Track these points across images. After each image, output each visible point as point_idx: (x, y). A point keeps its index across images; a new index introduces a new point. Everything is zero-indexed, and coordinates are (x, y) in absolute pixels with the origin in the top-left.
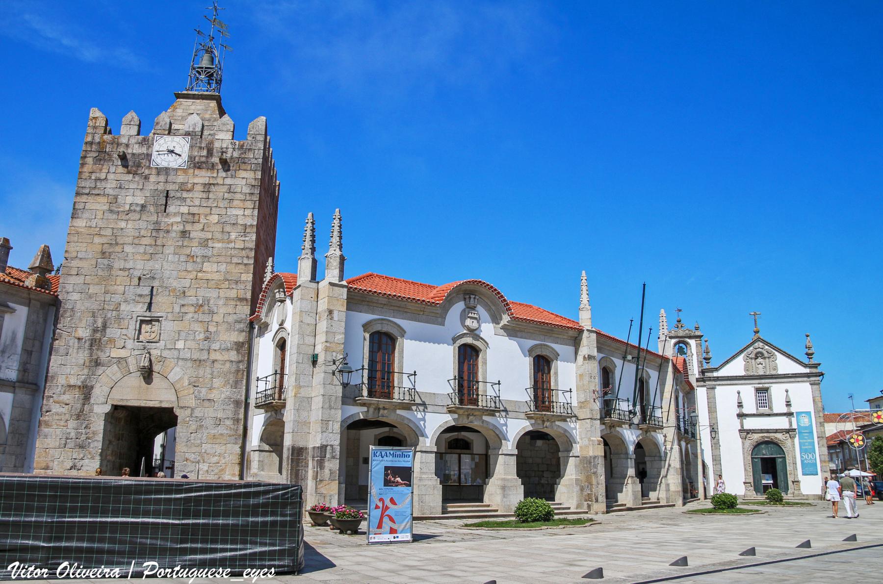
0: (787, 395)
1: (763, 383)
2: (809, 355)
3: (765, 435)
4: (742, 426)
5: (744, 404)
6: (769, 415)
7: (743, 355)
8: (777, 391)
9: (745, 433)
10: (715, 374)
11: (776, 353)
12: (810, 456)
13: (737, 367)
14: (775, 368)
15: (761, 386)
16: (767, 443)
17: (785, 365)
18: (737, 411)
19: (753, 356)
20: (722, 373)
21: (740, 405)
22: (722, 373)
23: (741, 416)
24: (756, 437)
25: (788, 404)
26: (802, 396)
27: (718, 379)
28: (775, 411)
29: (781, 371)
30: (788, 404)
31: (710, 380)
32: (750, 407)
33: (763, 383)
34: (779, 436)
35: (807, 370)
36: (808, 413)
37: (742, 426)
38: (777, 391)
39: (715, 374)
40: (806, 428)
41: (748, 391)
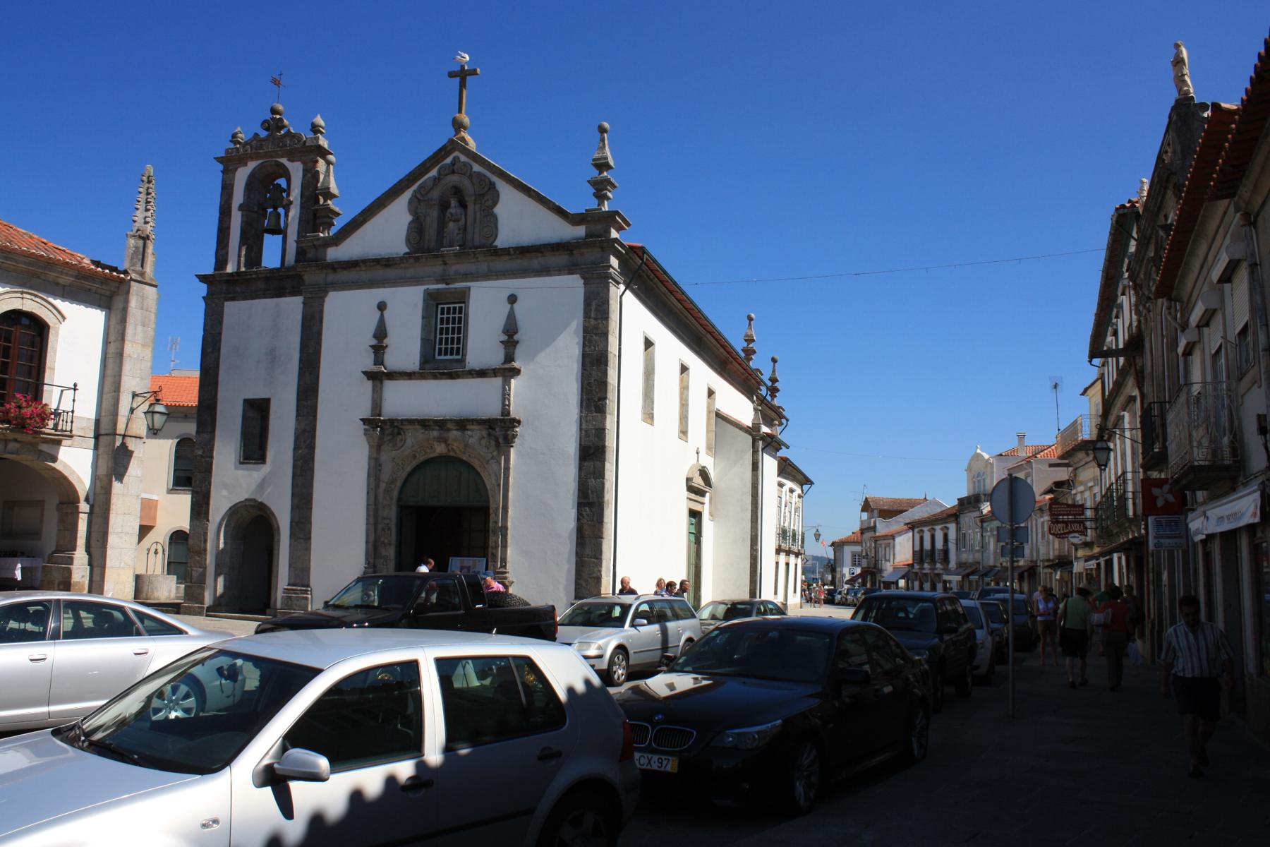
0: (511, 318)
2: (600, 188)
4: (377, 405)
6: (452, 376)
7: (408, 194)
9: (382, 429)
11: (502, 186)
19: (435, 194)
23: (377, 377)
32: (405, 349)
37: (377, 405)
41: (406, 306)
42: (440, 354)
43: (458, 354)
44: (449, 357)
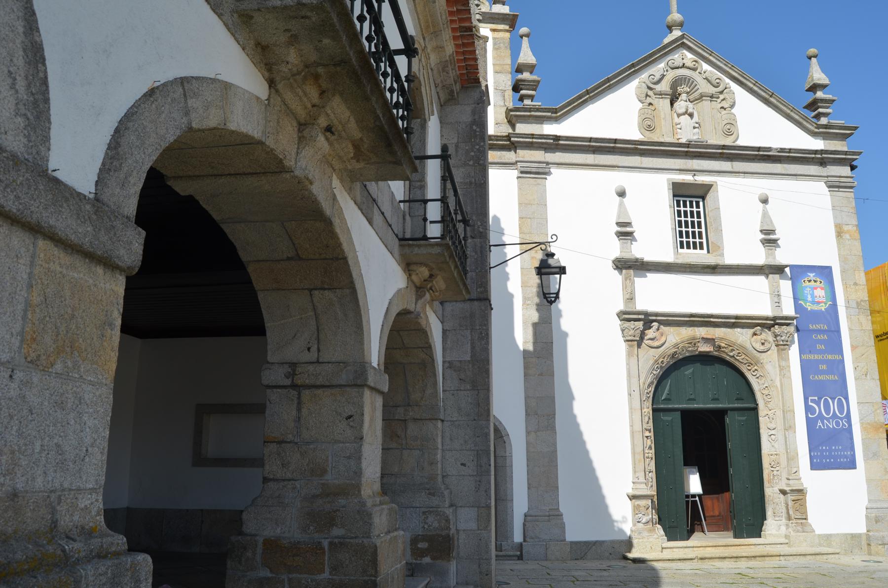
0: (765, 215)
1: (694, 171)
3: (702, 332)
5: (636, 228)
8: (736, 199)
10: (550, 129)
12: (834, 406)
13: (615, 114)
14: (730, 129)
15: (688, 178)
16: (705, 359)
17: (759, 124)
18: (615, 249)
19: (664, 86)
20: (574, 126)
21: (625, 234)
22: (574, 126)
24: (674, 339)
25: (770, 241)
26: (807, 218)
27: (556, 144)
28: (730, 258)
29: (746, 138)
30: (770, 241)
31: (530, 146)
32: (657, 240)
33: (694, 171)
34: (741, 336)
35: (818, 144)
36: (825, 272)
38: (736, 199)
39: (550, 129)
40: (816, 316)
41: (649, 193)
42: (682, 247)
43: (701, 248)
44: (692, 251)
